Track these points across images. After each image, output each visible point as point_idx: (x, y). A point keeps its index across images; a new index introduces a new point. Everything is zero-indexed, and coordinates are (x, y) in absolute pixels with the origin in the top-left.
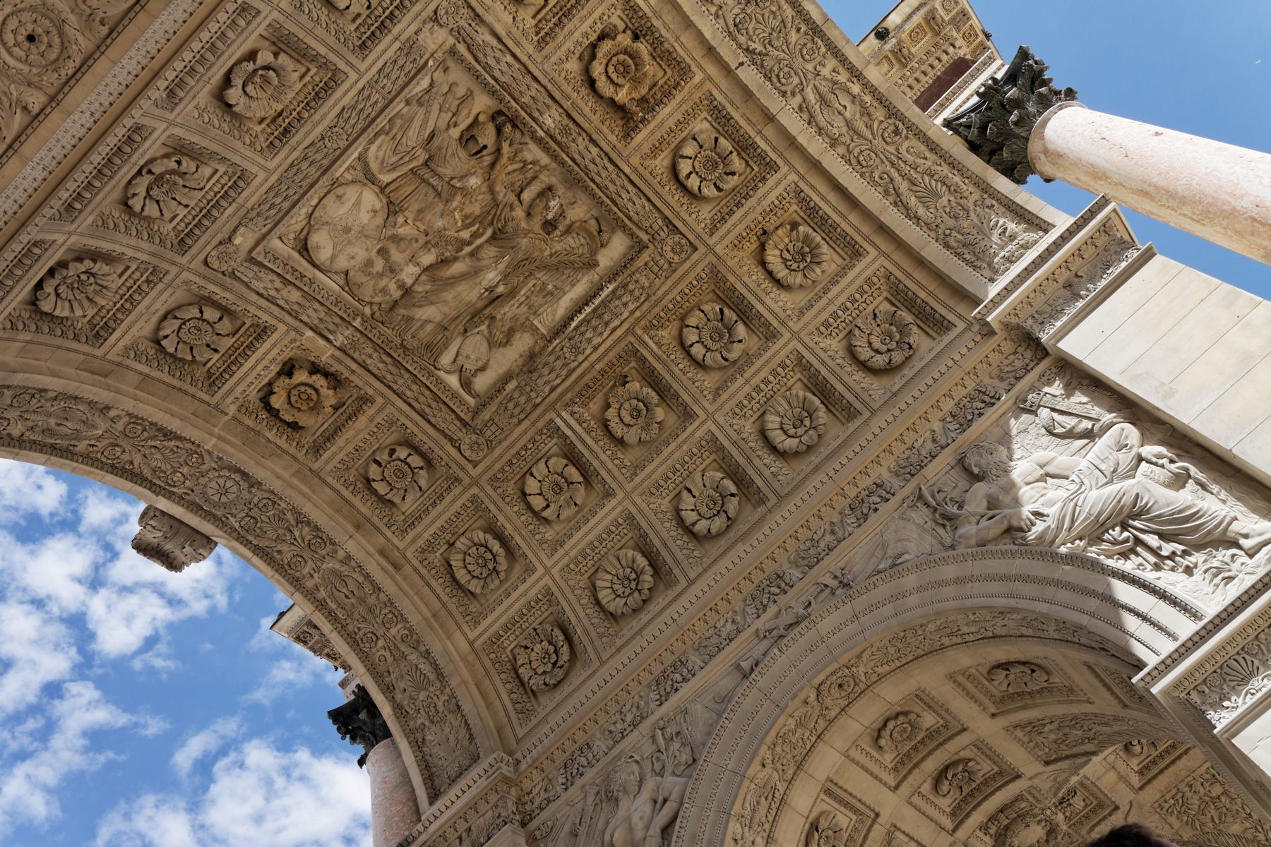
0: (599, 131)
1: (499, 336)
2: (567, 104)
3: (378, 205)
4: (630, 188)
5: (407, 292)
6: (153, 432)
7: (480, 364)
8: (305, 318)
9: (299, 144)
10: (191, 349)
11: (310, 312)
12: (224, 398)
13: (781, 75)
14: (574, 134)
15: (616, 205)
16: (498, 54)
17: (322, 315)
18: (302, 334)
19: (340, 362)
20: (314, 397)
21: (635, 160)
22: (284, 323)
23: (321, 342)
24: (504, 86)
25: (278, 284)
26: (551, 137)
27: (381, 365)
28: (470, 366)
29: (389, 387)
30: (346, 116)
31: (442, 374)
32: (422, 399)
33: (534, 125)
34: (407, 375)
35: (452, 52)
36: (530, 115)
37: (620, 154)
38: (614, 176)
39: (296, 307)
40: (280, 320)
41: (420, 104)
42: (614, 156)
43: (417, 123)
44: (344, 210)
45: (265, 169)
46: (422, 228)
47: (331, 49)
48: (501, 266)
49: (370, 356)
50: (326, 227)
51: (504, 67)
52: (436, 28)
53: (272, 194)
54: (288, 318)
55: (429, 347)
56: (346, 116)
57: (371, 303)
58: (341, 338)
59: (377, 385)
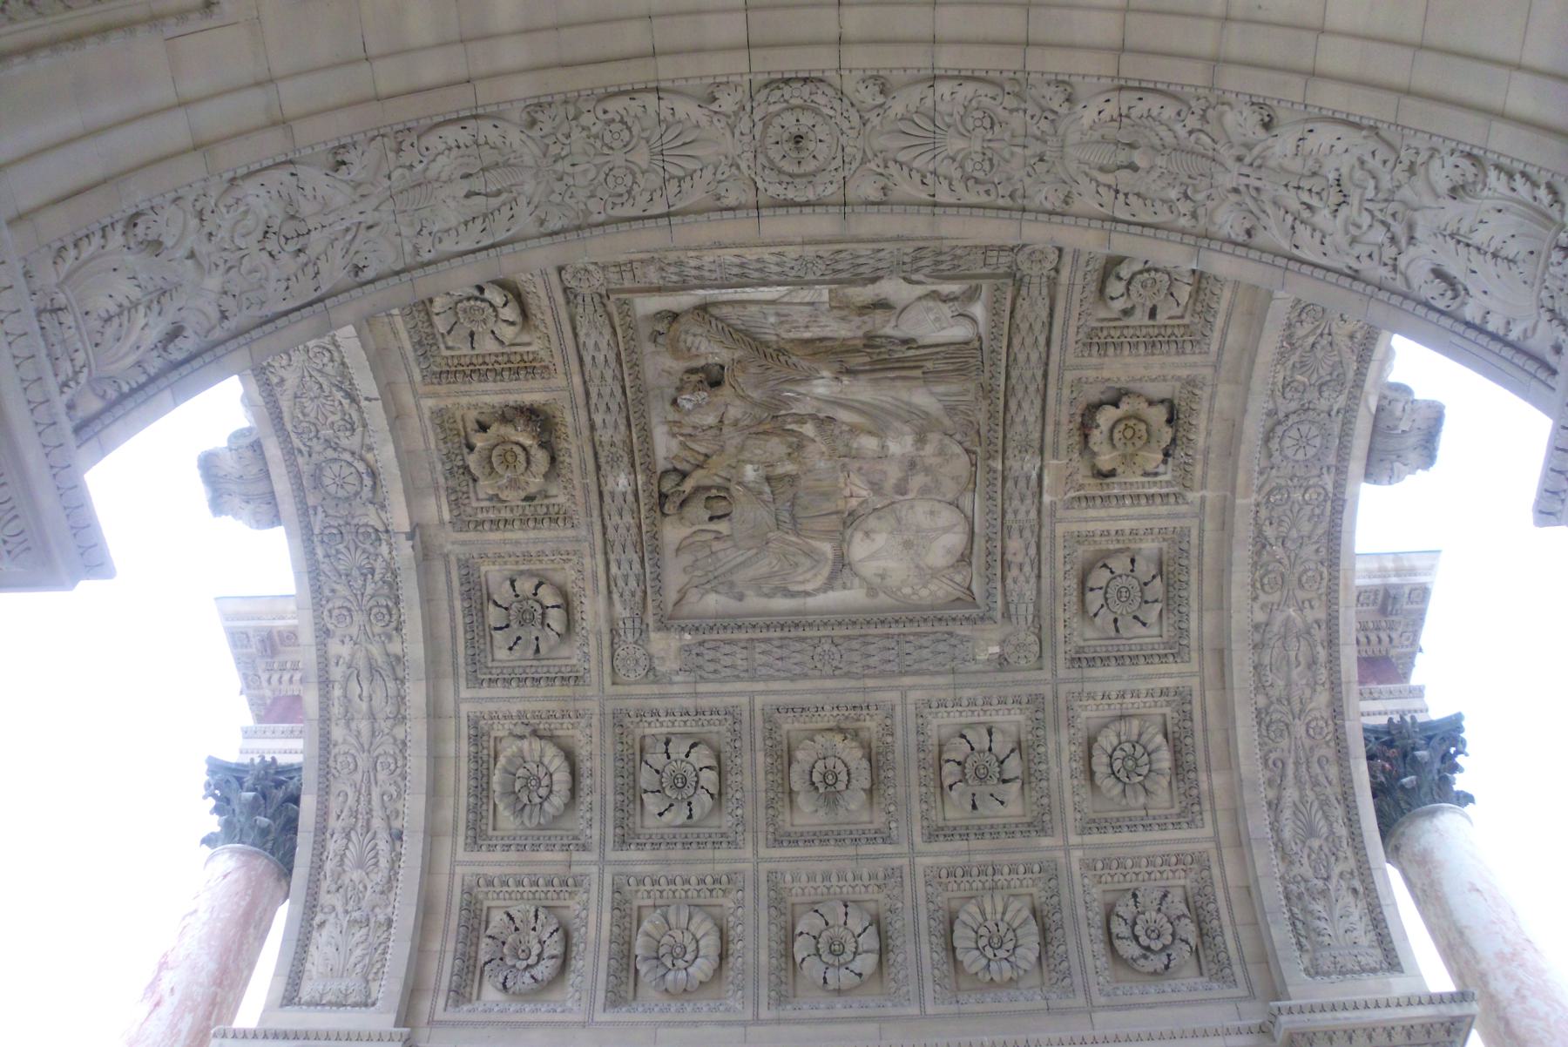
0: (578, 432)
1: (879, 315)
2: (591, 480)
3: (859, 536)
4: (587, 359)
5: (921, 440)
6: (1265, 557)
7: (931, 304)
8: (1033, 514)
9: (857, 690)
10: (1146, 584)
11: (1021, 516)
12: (1184, 516)
13: (326, 360)
14: (607, 448)
15: (618, 355)
16: (621, 583)
17: (1016, 502)
18: (1053, 504)
19: (1056, 444)
20: (1121, 427)
21: (560, 381)
22: (1053, 531)
23: (1046, 481)
24: (639, 545)
25: (1014, 572)
26: (633, 465)
27: (1026, 405)
28: (946, 310)
29: (1045, 376)
30: (798, 670)
31: (982, 330)
32: (1029, 341)
33: (640, 492)
34: (1014, 374)
35: (664, 625)
36: (637, 500)
37: (572, 399)
38: (597, 381)
39: (1027, 533)
40: (1053, 538)
41: (732, 585)
42: (581, 400)
43: (750, 572)
44: (891, 564)
45: (904, 697)
46: (842, 477)
47: (753, 749)
48: (802, 389)
49: (1025, 421)
50: (922, 564)
51: (625, 566)
52: (656, 662)
53: (924, 665)
54: (1045, 532)
55: (961, 371)
56: (798, 670)
57: (967, 451)
58: (1027, 467)
59: (1052, 392)
